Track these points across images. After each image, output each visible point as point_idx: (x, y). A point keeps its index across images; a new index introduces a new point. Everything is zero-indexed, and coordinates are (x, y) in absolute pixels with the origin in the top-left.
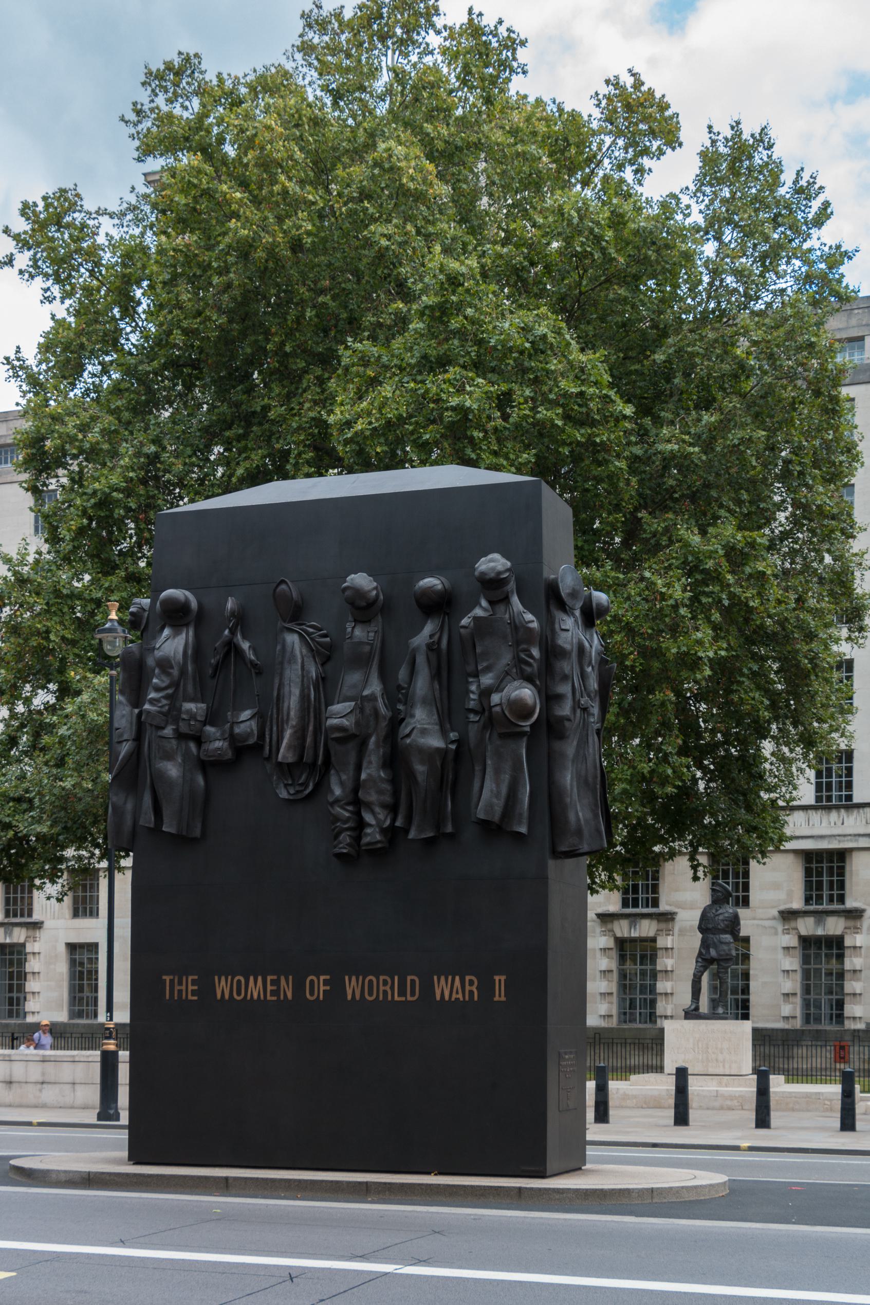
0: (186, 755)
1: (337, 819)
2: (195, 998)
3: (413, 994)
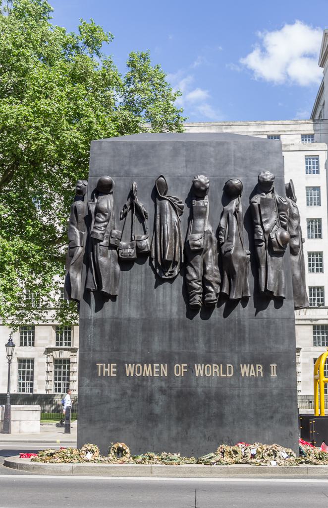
2: (115, 375)
3: (230, 373)
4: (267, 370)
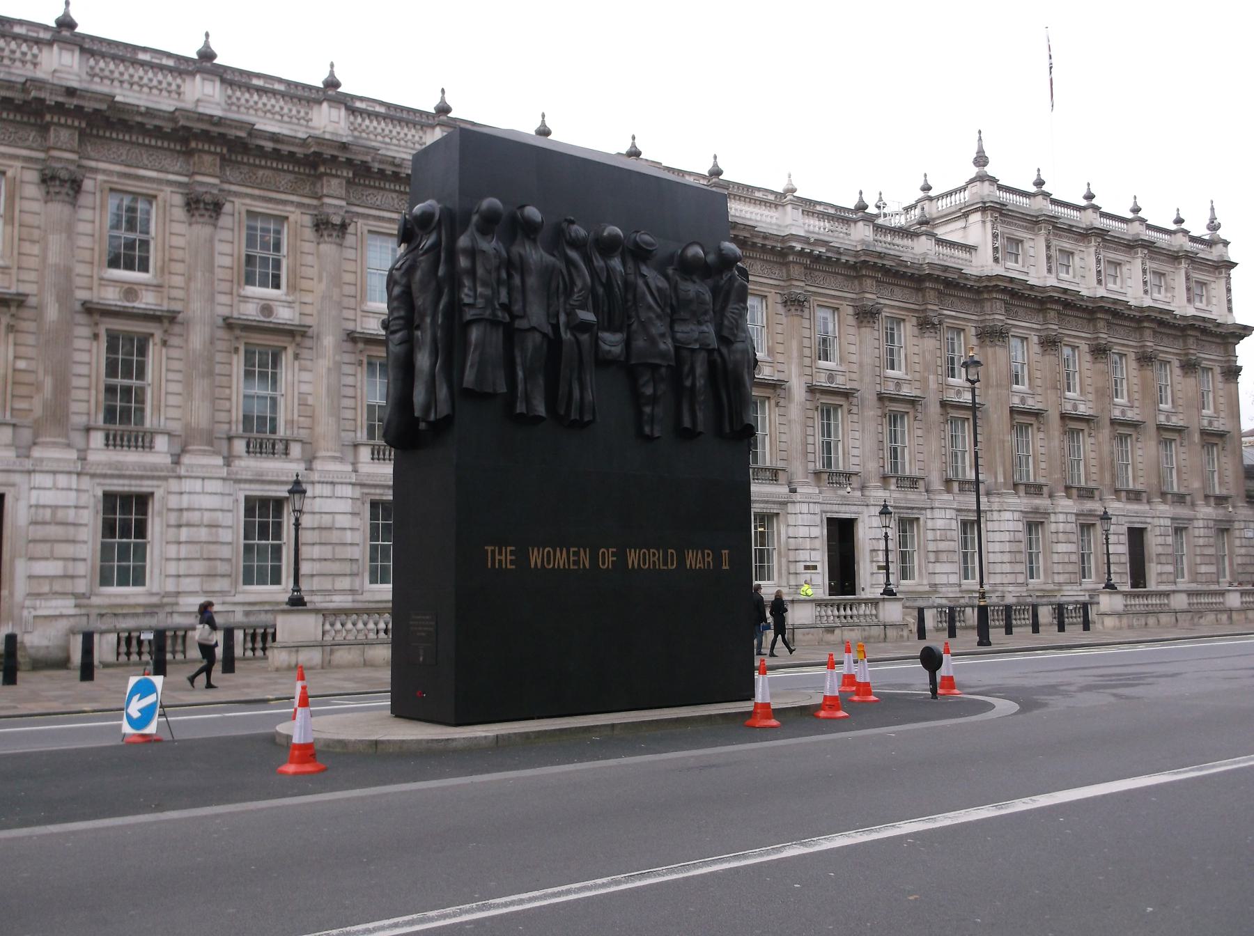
4: (718, 559)
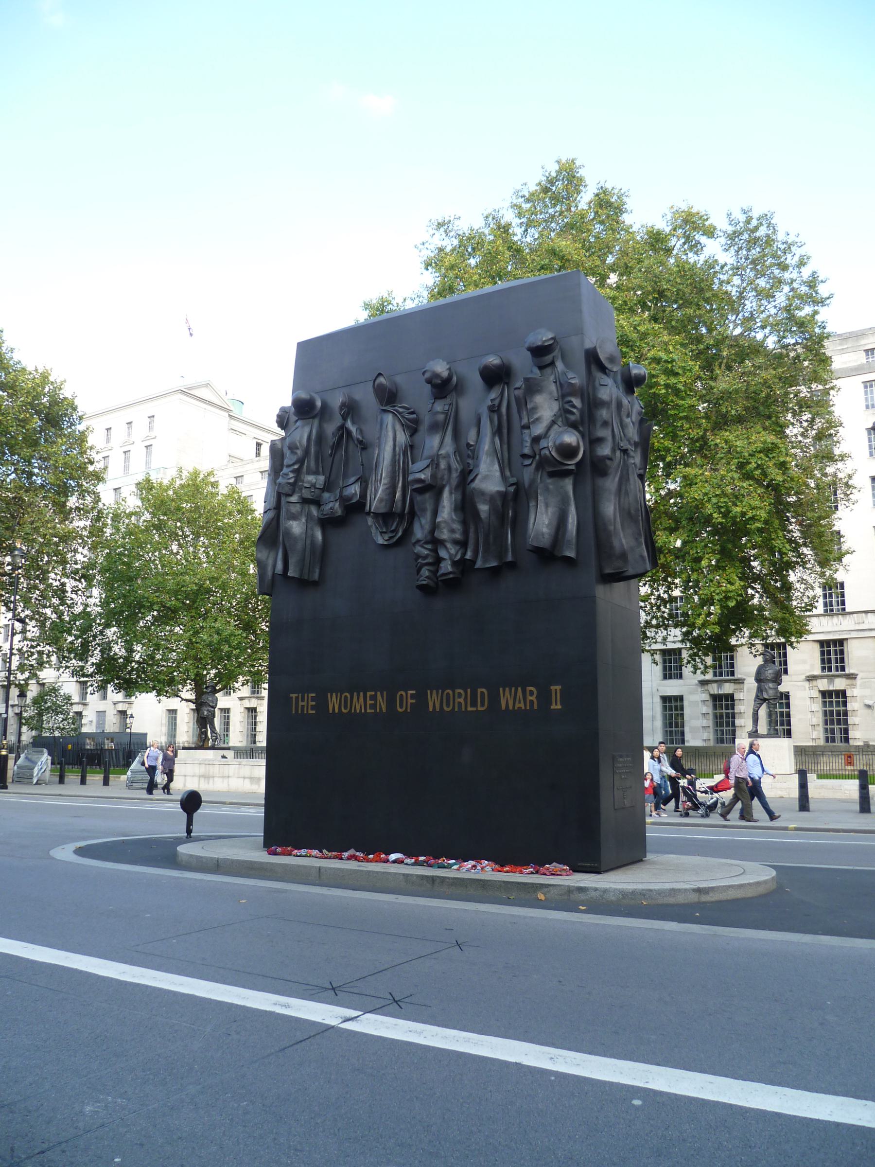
0: (309, 517)
1: (418, 556)
2: (314, 712)
3: (482, 705)
